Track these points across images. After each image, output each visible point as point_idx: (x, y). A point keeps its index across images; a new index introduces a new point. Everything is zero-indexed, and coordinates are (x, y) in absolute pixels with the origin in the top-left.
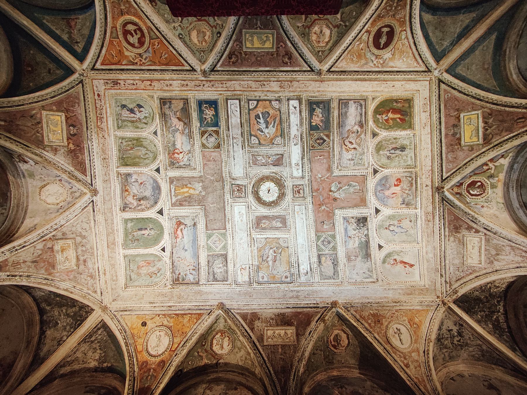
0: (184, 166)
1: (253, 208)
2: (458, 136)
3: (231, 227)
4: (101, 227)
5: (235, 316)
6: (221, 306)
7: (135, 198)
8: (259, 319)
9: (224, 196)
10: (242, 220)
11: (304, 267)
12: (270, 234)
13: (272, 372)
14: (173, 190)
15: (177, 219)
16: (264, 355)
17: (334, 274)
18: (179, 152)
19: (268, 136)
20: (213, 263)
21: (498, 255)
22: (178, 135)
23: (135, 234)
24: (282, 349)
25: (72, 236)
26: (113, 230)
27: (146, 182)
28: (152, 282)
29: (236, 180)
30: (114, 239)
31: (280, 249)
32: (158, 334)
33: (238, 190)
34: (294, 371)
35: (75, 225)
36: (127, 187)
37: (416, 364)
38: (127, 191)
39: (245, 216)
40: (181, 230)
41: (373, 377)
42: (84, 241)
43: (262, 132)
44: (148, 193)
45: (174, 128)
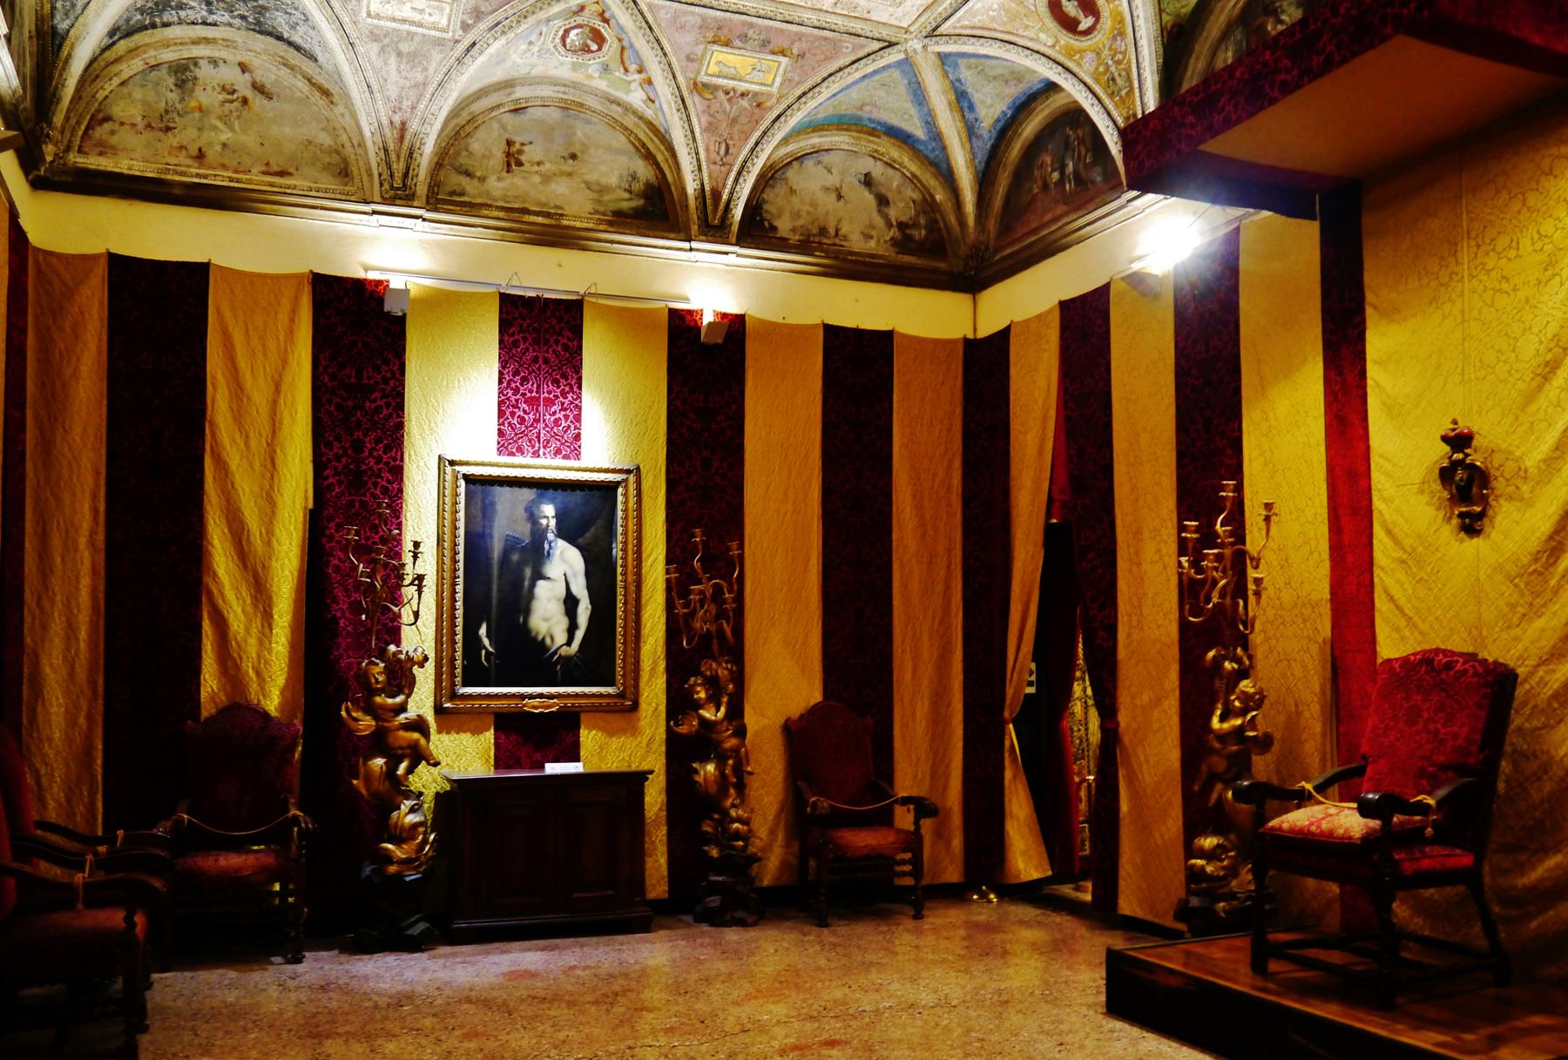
2: (737, 43)
21: (400, 54)
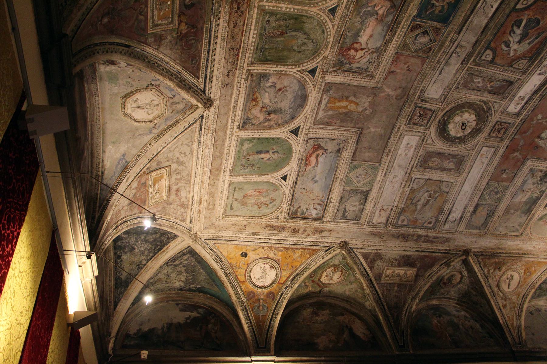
0: (357, 70)
1: (429, 141)
3: (388, 161)
4: (207, 151)
5: (356, 255)
6: (344, 245)
7: (264, 110)
8: (382, 259)
9: (397, 119)
10: (406, 155)
11: (455, 215)
12: (434, 175)
13: (386, 307)
14: (324, 102)
15: (315, 141)
16: (379, 292)
17: (482, 225)
18: (359, 48)
19: (511, 55)
20: (348, 199)
22: (371, 22)
23: (251, 158)
24: (398, 287)
25: (167, 164)
26: (222, 154)
27: (287, 89)
28: (259, 213)
29: (426, 102)
30: (221, 165)
31: (439, 193)
32: (263, 266)
33: (421, 115)
34: (406, 307)
35: (172, 149)
36: (257, 94)
37: (512, 305)
38: (254, 100)
39: (412, 150)
40: (317, 156)
41: (467, 308)
42: (181, 167)
43: (508, 46)
44: (286, 104)
45: (369, 9)
